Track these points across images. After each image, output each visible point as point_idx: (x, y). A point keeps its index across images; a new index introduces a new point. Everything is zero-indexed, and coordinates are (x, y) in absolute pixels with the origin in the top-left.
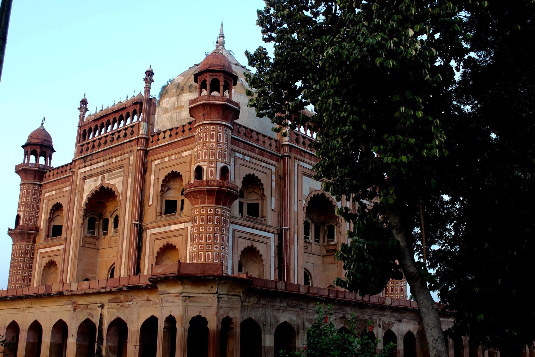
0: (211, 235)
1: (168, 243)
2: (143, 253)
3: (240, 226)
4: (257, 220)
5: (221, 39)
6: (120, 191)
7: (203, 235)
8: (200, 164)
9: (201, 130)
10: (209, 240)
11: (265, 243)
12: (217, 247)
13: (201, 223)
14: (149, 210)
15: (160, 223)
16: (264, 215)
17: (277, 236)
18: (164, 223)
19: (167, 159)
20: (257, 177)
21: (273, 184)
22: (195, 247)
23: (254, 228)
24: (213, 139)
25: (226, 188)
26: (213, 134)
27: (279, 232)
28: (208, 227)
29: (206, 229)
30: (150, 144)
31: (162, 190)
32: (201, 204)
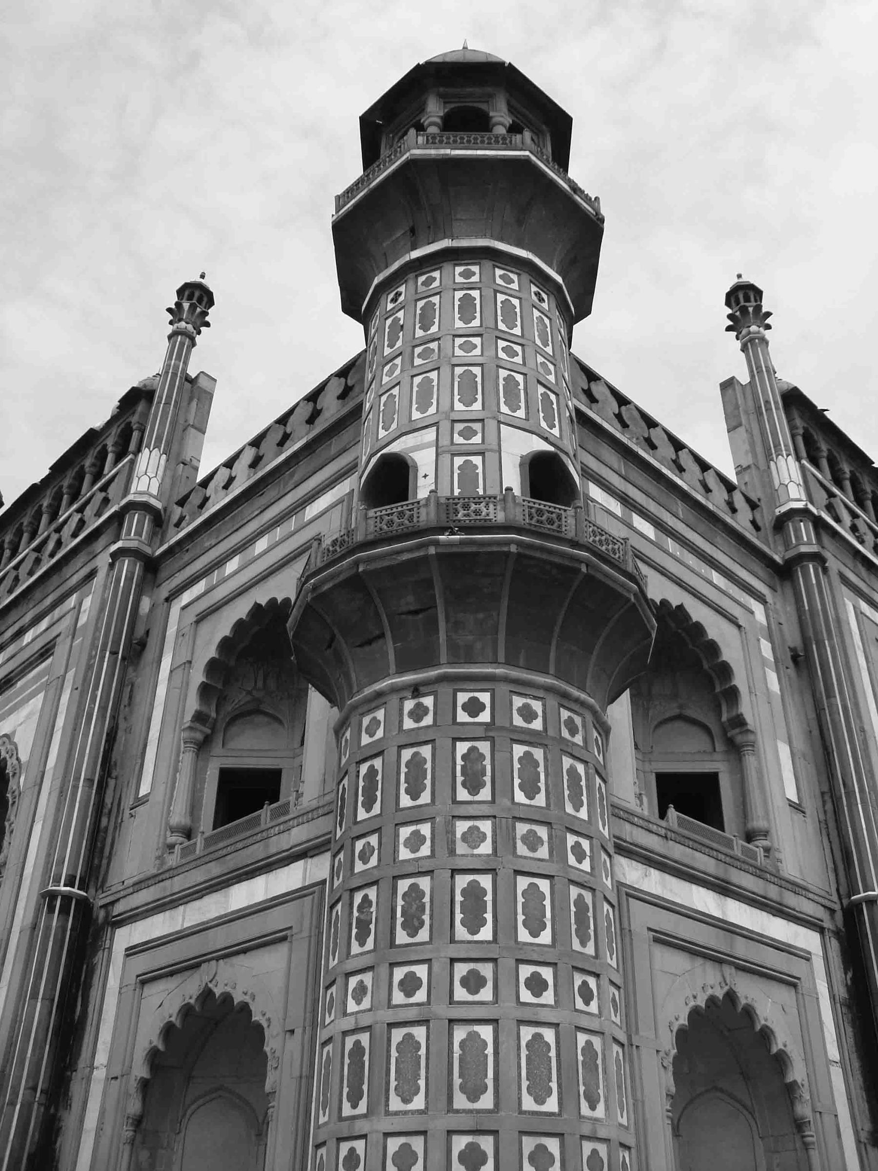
0: (485, 881)
1: (207, 994)
2: (82, 1063)
3: (655, 874)
4: (729, 844)
5: (471, 303)
6: (24, 758)
7: (425, 883)
8: (395, 448)
9: (394, 300)
10: (474, 924)
11: (792, 983)
12: (537, 985)
13: (406, 801)
14: (137, 821)
15: (178, 884)
16: (758, 823)
17: (834, 945)
18: (197, 876)
19: (231, 566)
20: (698, 629)
21: (772, 677)
22: (361, 990)
23: (724, 889)
24: (467, 318)
25: (575, 544)
26: (467, 301)
27: (839, 916)
28: (462, 827)
29: (445, 839)
30: (171, 529)
31: (199, 717)
32: (401, 671)
